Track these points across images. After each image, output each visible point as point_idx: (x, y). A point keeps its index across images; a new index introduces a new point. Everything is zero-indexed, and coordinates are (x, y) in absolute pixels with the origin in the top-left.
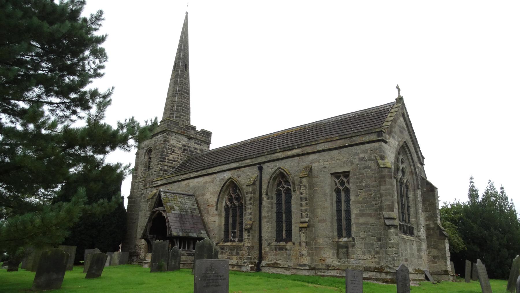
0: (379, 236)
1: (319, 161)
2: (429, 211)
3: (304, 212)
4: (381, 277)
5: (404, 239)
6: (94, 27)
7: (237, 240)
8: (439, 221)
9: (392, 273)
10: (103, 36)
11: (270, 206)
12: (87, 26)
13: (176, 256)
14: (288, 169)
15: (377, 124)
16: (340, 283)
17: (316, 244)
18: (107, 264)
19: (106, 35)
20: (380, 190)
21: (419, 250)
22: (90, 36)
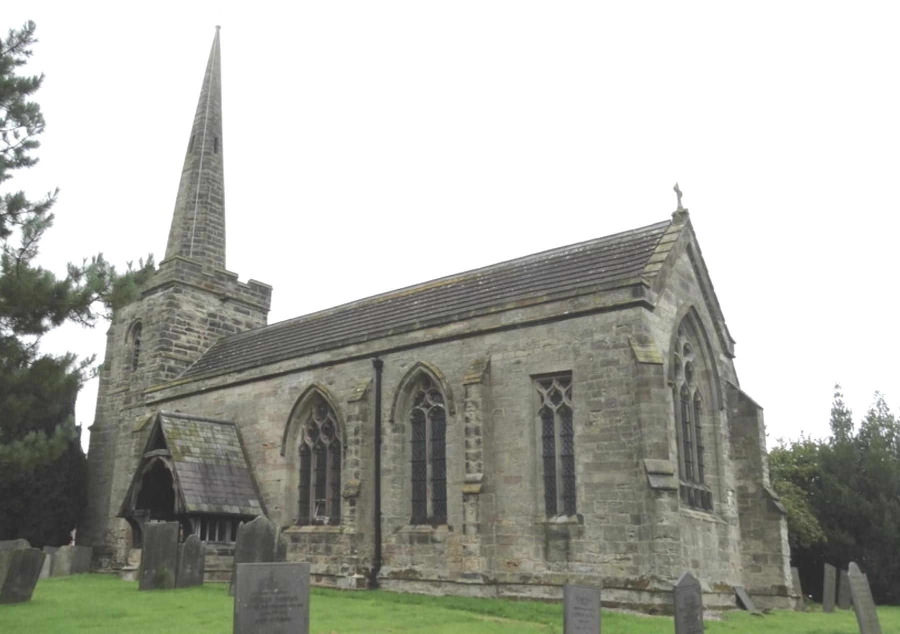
0: (636, 513)
1: (505, 349)
2: (745, 458)
3: (473, 460)
4: (640, 600)
5: (692, 518)
6: (15, 57)
7: (326, 520)
8: (766, 480)
9: (665, 591)
10: (35, 78)
11: (399, 446)
12: (2, 55)
13: (195, 555)
14: (438, 365)
15: (632, 268)
16: (551, 613)
17: (498, 528)
18: (45, 572)
19: (42, 76)
20: (637, 412)
21: (723, 543)
22: (7, 77)
